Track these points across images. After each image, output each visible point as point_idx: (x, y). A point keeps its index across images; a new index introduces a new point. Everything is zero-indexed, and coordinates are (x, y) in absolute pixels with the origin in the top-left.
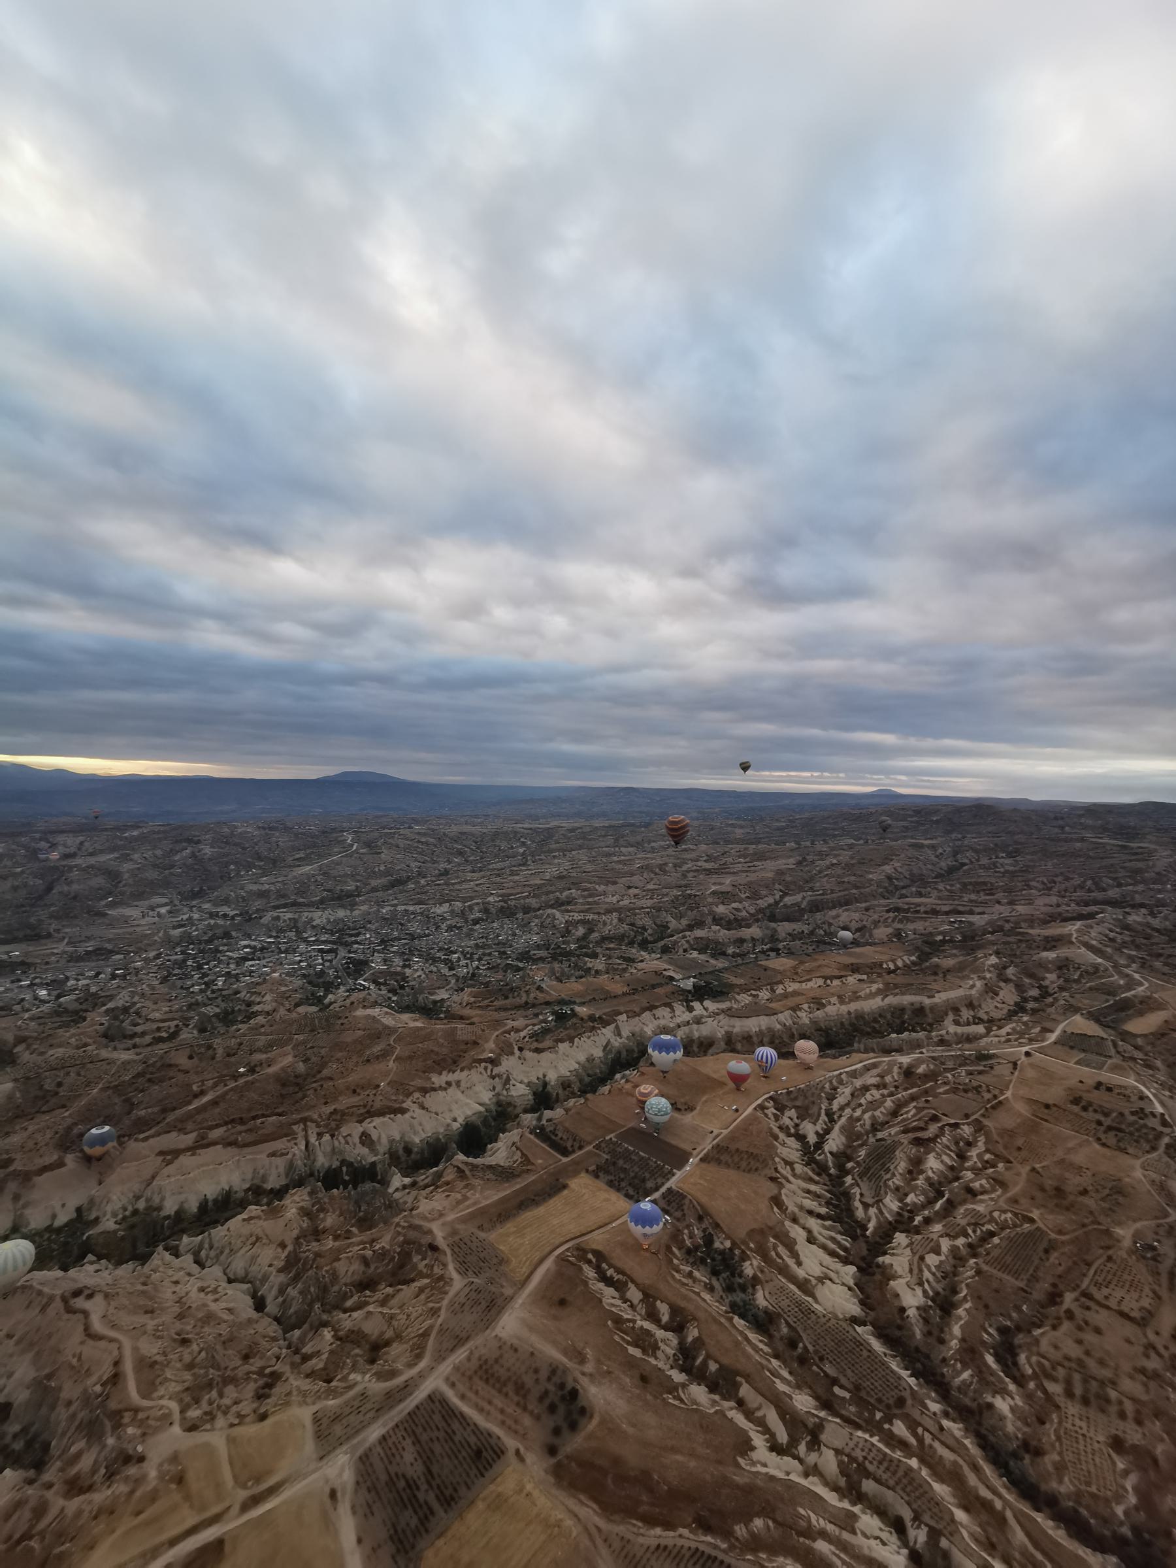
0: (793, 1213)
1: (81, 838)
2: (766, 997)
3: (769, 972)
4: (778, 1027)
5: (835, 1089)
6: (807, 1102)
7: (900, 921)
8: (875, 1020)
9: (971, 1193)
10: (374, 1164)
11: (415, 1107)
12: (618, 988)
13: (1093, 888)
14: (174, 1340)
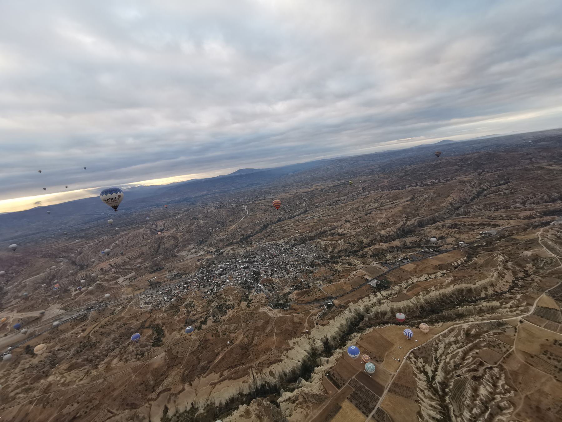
1: (164, 222)
2: (405, 286)
3: (405, 273)
4: (411, 305)
5: (437, 344)
7: (458, 233)
8: (451, 296)
9: (501, 409)
10: (275, 383)
12: (348, 288)
13: (548, 199)
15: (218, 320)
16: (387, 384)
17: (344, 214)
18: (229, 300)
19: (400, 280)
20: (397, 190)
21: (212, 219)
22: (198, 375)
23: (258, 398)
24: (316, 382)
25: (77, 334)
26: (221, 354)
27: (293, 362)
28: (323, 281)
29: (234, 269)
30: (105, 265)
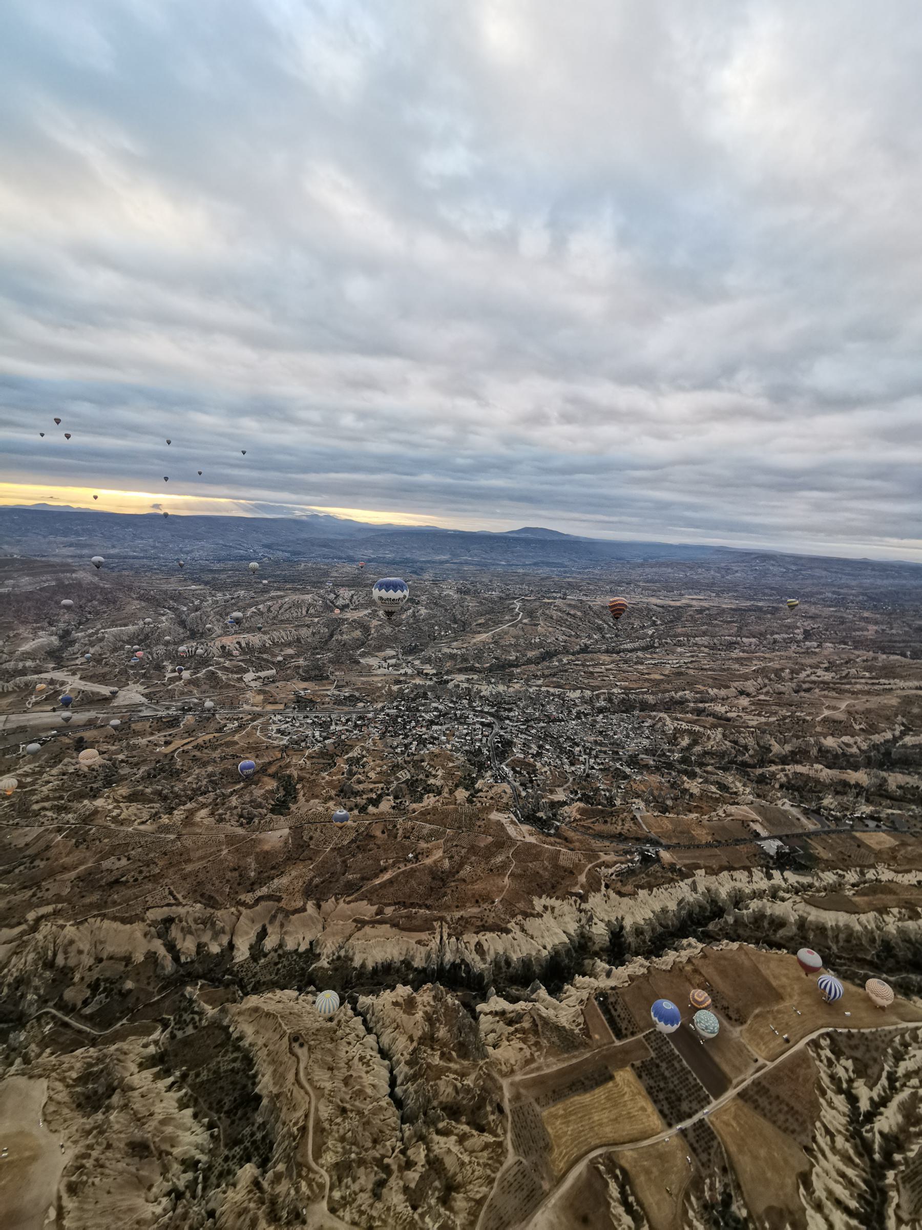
0: (820, 1200)
1: (353, 592)
2: (852, 881)
3: (863, 850)
4: (858, 928)
5: (906, 1045)
6: (868, 1056)
10: (483, 970)
11: (516, 929)
12: (702, 835)
14: (339, 1106)
15: (402, 807)
16: (740, 1078)
17: (740, 676)
18: (435, 776)
19: (842, 863)
20: (899, 657)
21: (446, 610)
22: (336, 894)
23: (438, 984)
24: (572, 1004)
25: (155, 745)
26: (390, 872)
27: (532, 944)
28: (647, 802)
29: (462, 720)
30: (230, 641)
